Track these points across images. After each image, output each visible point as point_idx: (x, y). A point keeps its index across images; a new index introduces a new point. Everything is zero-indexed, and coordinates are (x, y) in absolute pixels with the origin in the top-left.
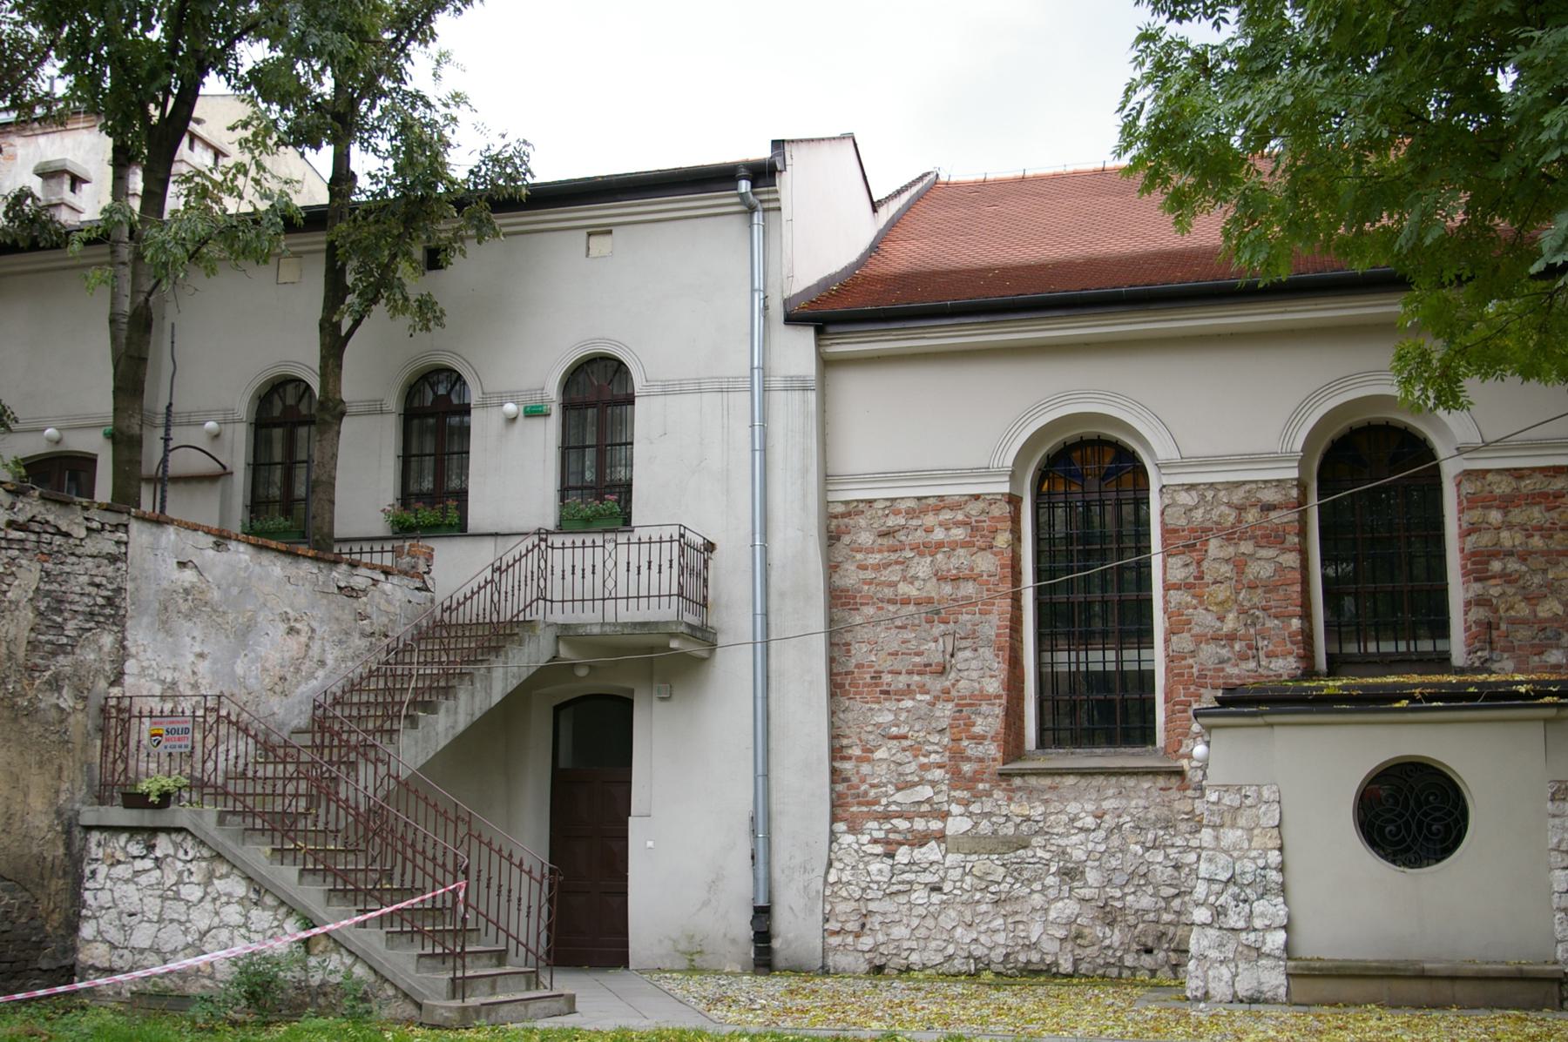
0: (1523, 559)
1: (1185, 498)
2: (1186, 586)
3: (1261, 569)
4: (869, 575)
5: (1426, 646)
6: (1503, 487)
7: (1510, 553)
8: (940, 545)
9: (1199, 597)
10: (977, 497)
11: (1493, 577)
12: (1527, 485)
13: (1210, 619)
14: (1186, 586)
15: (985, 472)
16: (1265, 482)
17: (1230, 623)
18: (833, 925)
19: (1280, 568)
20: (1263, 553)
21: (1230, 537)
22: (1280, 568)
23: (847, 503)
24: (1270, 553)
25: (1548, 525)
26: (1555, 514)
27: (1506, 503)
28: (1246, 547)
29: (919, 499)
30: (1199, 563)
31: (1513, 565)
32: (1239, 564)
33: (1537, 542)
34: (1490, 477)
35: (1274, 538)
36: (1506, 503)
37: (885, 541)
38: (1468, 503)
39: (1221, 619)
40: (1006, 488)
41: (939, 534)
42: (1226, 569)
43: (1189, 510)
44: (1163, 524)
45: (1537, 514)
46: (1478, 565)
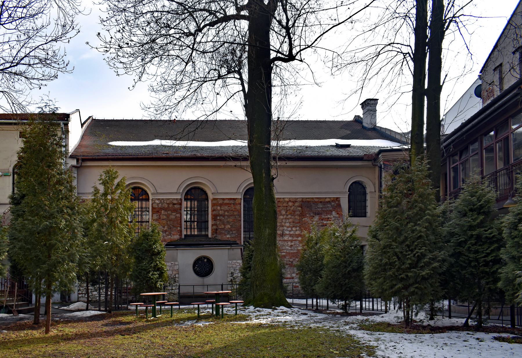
0: (224, 217)
1: (157, 202)
2: (157, 220)
3: (173, 217)
5: (203, 233)
6: (221, 202)
7: (221, 215)
9: (160, 223)
12: (225, 202)
13: (161, 227)
14: (157, 220)
17: (166, 228)
18: (80, 292)
19: (176, 217)
21: (166, 209)
24: (175, 214)
27: (221, 205)
30: (160, 215)
32: (168, 216)
33: (226, 213)
35: (175, 211)
36: (221, 205)
38: (213, 205)
39: (164, 227)
42: (165, 217)
43: (158, 204)
44: (152, 207)
45: (226, 208)
46: (215, 218)
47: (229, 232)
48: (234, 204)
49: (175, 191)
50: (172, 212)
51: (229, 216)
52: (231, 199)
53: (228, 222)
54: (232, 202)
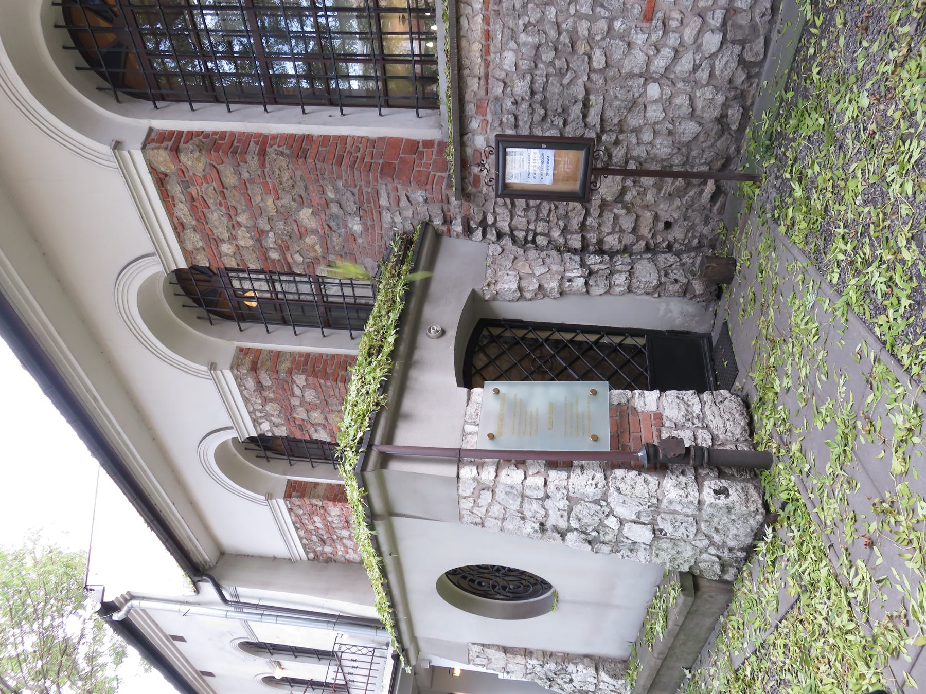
4: (350, 551)
8: (326, 526)
10: (290, 510)
11: (285, 258)
12: (189, 221)
15: (272, 509)
16: (239, 386)
19: (307, 386)
20: (297, 392)
22: (307, 386)
23: (307, 553)
25: (223, 209)
26: (210, 202)
28: (295, 402)
29: (297, 529)
31: (270, 240)
33: (243, 218)
34: (190, 247)
35: (285, 387)
37: (328, 542)
40: (281, 502)
41: (319, 525)
45: (216, 218)
47: (333, 217)
48: (186, 185)
49: (211, 384)
50: (293, 394)
51: (257, 212)
52: (165, 196)
53: (286, 215)
54: (176, 189)
